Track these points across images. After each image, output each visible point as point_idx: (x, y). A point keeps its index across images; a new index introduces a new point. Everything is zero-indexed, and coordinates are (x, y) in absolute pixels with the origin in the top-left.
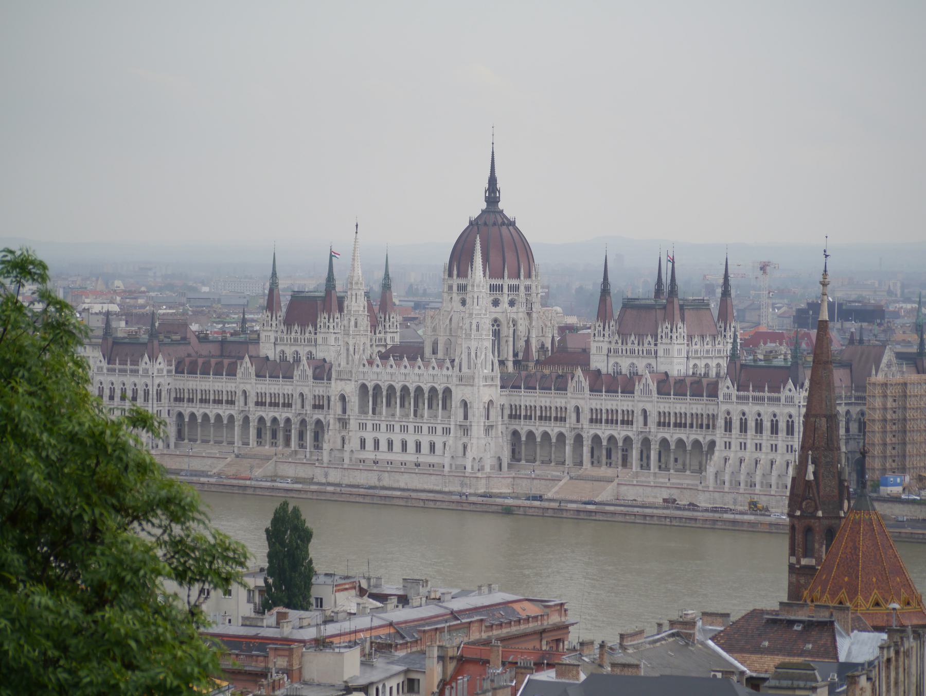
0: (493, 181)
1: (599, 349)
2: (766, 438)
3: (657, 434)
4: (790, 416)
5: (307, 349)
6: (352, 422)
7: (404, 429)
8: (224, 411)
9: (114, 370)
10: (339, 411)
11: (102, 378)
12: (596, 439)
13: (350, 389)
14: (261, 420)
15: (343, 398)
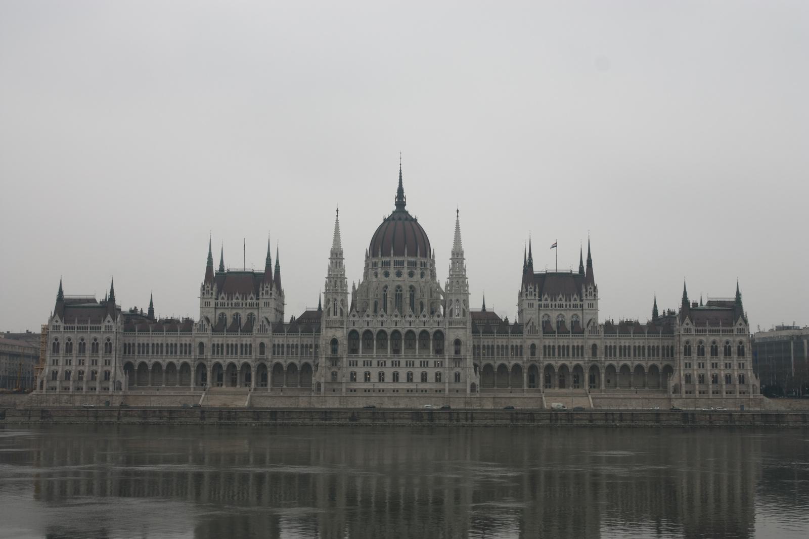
0: (400, 191)
1: (531, 305)
2: (721, 360)
3: (604, 361)
4: (741, 343)
5: (249, 311)
6: (345, 360)
7: (396, 364)
8: (178, 361)
9: (73, 328)
10: (329, 352)
11: (58, 335)
12: (549, 367)
13: (341, 335)
14: (218, 366)
15: (334, 342)
